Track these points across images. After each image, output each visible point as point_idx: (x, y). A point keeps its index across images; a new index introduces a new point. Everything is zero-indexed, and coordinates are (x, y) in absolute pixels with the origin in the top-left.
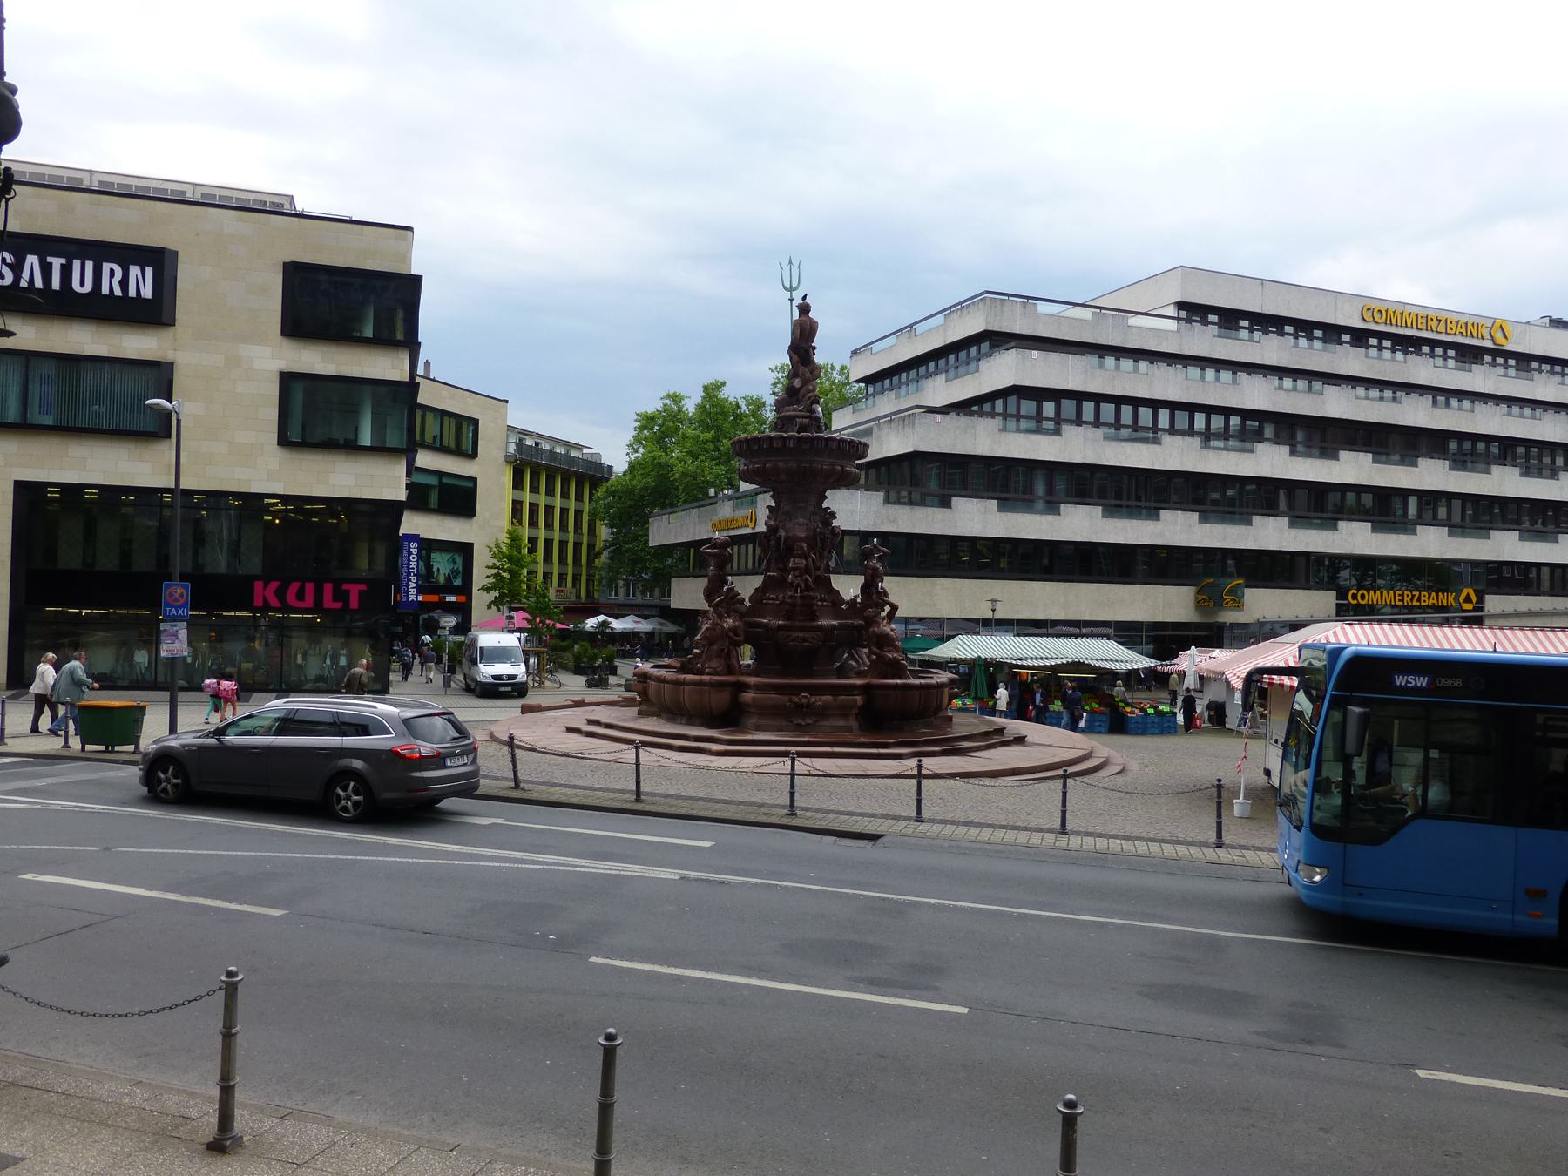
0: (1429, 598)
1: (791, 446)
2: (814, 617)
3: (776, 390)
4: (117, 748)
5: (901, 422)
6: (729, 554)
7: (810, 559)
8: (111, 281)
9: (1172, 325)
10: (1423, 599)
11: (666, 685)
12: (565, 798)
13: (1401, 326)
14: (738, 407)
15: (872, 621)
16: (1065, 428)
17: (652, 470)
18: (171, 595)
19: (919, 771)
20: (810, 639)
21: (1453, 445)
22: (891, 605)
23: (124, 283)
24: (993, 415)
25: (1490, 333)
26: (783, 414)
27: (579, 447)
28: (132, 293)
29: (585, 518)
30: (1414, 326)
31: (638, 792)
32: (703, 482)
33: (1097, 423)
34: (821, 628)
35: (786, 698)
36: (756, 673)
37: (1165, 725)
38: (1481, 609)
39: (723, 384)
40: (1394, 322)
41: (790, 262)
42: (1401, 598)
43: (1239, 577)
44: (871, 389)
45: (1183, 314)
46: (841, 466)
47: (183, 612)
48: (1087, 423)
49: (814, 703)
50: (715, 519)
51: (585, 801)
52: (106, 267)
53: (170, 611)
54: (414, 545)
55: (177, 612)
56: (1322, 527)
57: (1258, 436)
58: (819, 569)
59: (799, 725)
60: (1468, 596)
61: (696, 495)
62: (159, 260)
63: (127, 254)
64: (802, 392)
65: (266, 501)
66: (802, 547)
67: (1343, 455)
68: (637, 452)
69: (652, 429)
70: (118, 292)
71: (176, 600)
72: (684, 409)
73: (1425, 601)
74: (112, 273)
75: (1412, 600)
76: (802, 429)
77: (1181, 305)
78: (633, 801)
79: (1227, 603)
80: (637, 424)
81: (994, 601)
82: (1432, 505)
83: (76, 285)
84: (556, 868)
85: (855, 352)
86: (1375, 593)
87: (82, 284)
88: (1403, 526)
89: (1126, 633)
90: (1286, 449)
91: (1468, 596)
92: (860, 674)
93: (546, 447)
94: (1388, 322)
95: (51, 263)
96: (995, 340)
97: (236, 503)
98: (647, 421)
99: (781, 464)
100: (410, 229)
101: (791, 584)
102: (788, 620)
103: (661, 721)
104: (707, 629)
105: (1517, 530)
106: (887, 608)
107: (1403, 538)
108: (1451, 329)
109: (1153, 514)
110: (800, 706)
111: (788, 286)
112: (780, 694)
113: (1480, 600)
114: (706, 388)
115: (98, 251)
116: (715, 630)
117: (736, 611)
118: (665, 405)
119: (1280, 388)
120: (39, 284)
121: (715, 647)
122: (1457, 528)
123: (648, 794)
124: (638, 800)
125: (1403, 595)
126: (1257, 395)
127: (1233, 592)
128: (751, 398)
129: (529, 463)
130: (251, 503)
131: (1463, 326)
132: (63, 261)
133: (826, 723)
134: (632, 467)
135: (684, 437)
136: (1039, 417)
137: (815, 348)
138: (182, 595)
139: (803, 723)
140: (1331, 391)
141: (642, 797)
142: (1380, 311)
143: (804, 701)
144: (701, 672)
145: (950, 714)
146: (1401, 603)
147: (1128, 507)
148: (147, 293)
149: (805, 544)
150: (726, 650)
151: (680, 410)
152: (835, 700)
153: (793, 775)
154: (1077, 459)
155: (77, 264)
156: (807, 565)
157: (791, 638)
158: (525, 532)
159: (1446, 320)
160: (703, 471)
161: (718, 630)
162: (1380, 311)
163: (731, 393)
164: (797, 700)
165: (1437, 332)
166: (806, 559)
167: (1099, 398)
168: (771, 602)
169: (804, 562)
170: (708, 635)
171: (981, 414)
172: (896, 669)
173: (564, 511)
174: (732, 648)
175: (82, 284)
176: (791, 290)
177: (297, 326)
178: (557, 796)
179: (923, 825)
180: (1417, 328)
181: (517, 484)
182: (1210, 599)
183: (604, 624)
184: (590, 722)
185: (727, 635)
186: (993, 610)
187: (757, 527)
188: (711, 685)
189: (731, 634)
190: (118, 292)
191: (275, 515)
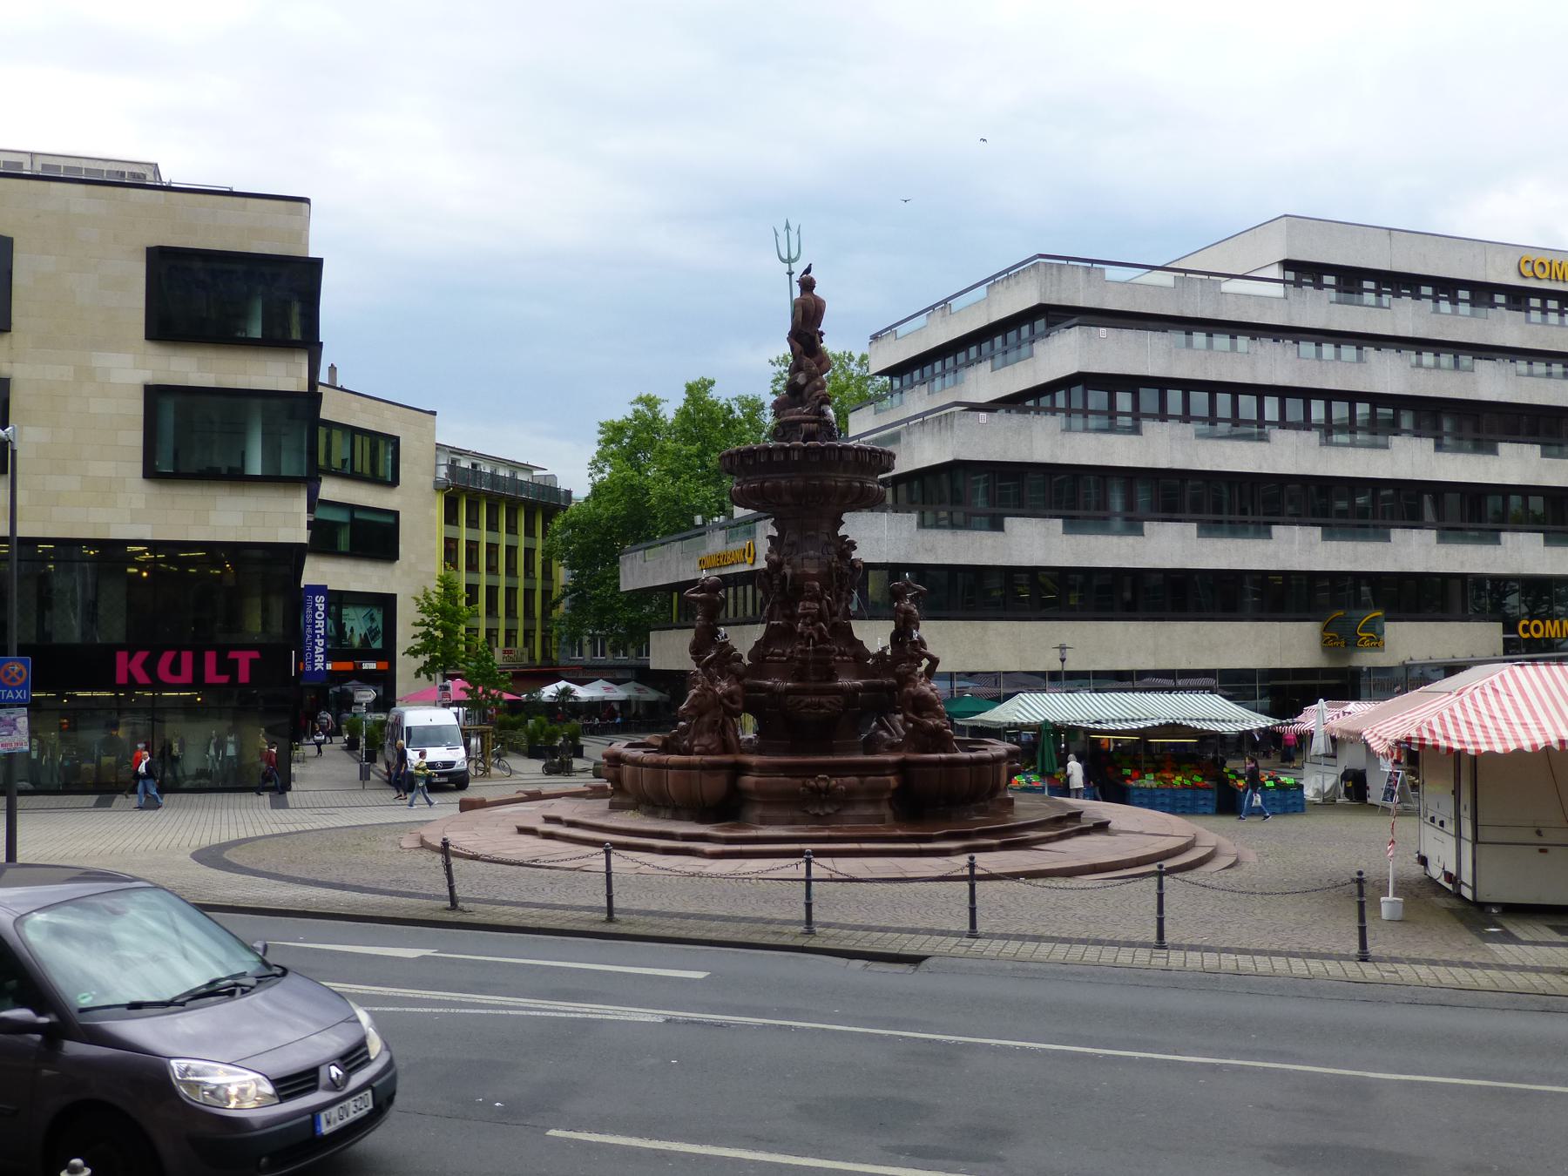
1: (796, 458)
2: (831, 675)
3: (778, 388)
5: (936, 423)
6: (721, 598)
7: (824, 602)
9: (1277, 290)
11: (644, 769)
14: (731, 411)
15: (906, 679)
16: (1146, 424)
17: (622, 494)
18: (7, 673)
19: (972, 871)
20: (828, 705)
22: (930, 657)
24: (1053, 410)
26: (784, 419)
27: (528, 468)
29: (539, 558)
31: (610, 909)
32: (687, 507)
33: (1186, 417)
34: (841, 690)
35: (799, 781)
36: (759, 751)
37: (1289, 802)
39: (712, 383)
40: (1560, 277)
41: (788, 227)
43: (1377, 607)
44: (897, 383)
45: (1291, 276)
46: (860, 482)
48: (1173, 417)
50: (704, 554)
51: (542, 924)
53: (6, 694)
54: (320, 600)
55: (15, 694)
57: (1394, 428)
59: (817, 815)
64: (807, 390)
65: (130, 549)
66: (814, 588)
69: (620, 442)
71: (13, 680)
72: (661, 415)
76: (810, 436)
77: (1287, 265)
79: (1363, 642)
80: (601, 437)
81: (1062, 648)
84: (504, 1012)
85: (875, 337)
86: (1552, 625)
89: (1235, 684)
90: (1429, 443)
92: (893, 748)
93: (486, 469)
94: (1553, 277)
96: (1053, 316)
97: (92, 553)
98: (614, 433)
99: (783, 482)
100: (306, 200)
101: (801, 634)
102: (799, 680)
103: (639, 816)
104: (695, 695)
106: (925, 662)
109: (1262, 530)
110: (816, 791)
111: (785, 257)
112: (791, 777)
114: (690, 389)
117: (731, 672)
118: (636, 411)
119: (1419, 365)
121: (706, 719)
123: (623, 911)
124: (610, 919)
128: (746, 399)
129: (465, 490)
130: (112, 551)
133: (851, 812)
134: (597, 491)
135: (662, 451)
136: (1112, 412)
137: (822, 334)
138: (20, 673)
139: (822, 814)
140: (1484, 367)
143: (822, 784)
144: (689, 752)
145: (1010, 796)
147: (1230, 522)
149: (817, 583)
150: (720, 721)
151: (655, 418)
152: (862, 782)
153: (808, 881)
154: (1163, 463)
156: (820, 610)
157: (802, 704)
158: (462, 578)
160: (687, 494)
161: (709, 697)
163: (721, 394)
164: (812, 783)
166: (819, 601)
167: (1187, 386)
168: (776, 658)
169: (817, 605)
170: (696, 703)
171: (1038, 410)
172: (938, 740)
173: (511, 550)
174: (727, 719)
176: (790, 261)
178: (506, 918)
181: (451, 518)
182: (1340, 638)
183: (566, 692)
184: (548, 820)
185: (721, 703)
186: (1063, 660)
187: (756, 562)
188: (703, 767)
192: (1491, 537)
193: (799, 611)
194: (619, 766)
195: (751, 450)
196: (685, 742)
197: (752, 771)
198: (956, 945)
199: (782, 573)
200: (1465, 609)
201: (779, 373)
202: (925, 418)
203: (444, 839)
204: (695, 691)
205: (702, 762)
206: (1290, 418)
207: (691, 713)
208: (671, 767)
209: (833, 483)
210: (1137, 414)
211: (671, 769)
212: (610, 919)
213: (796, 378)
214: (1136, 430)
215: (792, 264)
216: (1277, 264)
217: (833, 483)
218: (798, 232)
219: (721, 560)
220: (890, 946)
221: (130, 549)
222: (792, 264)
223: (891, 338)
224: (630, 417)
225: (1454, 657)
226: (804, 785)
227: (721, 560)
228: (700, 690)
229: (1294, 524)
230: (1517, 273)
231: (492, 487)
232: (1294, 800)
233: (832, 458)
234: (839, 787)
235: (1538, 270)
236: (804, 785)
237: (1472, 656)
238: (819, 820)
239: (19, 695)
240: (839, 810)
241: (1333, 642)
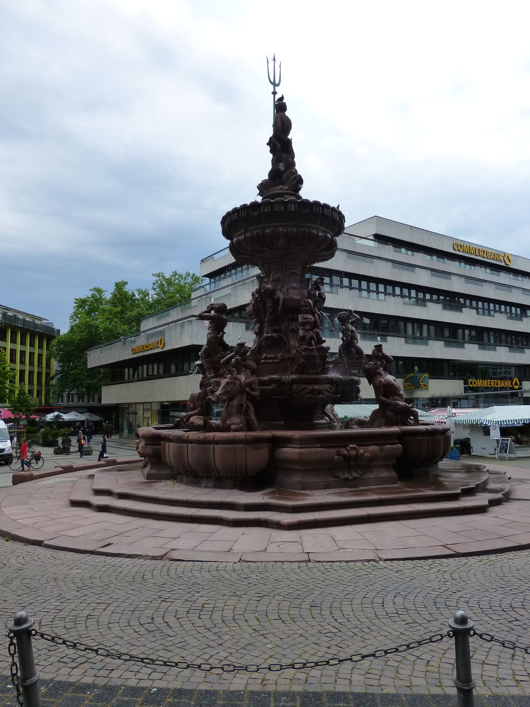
0: (501, 383)
1: (293, 209)
3: (155, 287)
5: (251, 284)
10: (499, 383)
11: (189, 445)
13: (469, 253)
14: (134, 295)
17: (85, 329)
25: (504, 259)
27: (40, 319)
30: (475, 254)
32: (117, 333)
34: (331, 381)
35: (333, 451)
37: (453, 455)
38: (520, 388)
39: (126, 283)
40: (466, 251)
42: (490, 383)
48: (346, 287)
50: (134, 346)
56: (457, 346)
59: (347, 479)
60: (516, 382)
68: (75, 321)
69: (84, 308)
72: (104, 297)
73: (499, 385)
75: (494, 384)
79: (421, 387)
80: (76, 305)
85: (202, 261)
86: (485, 381)
91: (516, 382)
93: (21, 317)
94: (464, 251)
98: (81, 303)
99: (280, 229)
103: (183, 487)
107: (492, 353)
108: (489, 256)
110: (347, 459)
112: (326, 447)
113: (521, 384)
114: (117, 285)
118: (93, 294)
128: (141, 291)
129: (10, 325)
131: (493, 255)
134: (72, 330)
135: (104, 310)
139: (350, 478)
142: (460, 246)
143: (353, 453)
146: (490, 386)
147: (371, 334)
151: (100, 298)
152: (382, 450)
159: (487, 252)
160: (116, 328)
162: (460, 246)
163: (129, 289)
164: (345, 452)
165: (483, 257)
168: (271, 361)
173: (32, 354)
180: (476, 255)
183: (58, 417)
184: (98, 492)
187: (165, 347)
188: (246, 442)
192: (461, 345)
194: (160, 444)
197: (291, 443)
199: (276, 297)
200: (449, 375)
201: (156, 280)
202: (244, 282)
203: (19, 621)
205: (248, 437)
207: (225, 397)
208: (191, 442)
211: (217, 444)
216: (372, 236)
219: (145, 348)
223: (212, 260)
224: (90, 296)
225: (448, 394)
226: (338, 454)
227: (145, 348)
228: (230, 378)
229: (395, 336)
230: (452, 246)
231: (23, 325)
232: (455, 455)
233: (318, 212)
235: (459, 248)
236: (338, 454)
237: (454, 394)
238: (347, 483)
241: (409, 387)
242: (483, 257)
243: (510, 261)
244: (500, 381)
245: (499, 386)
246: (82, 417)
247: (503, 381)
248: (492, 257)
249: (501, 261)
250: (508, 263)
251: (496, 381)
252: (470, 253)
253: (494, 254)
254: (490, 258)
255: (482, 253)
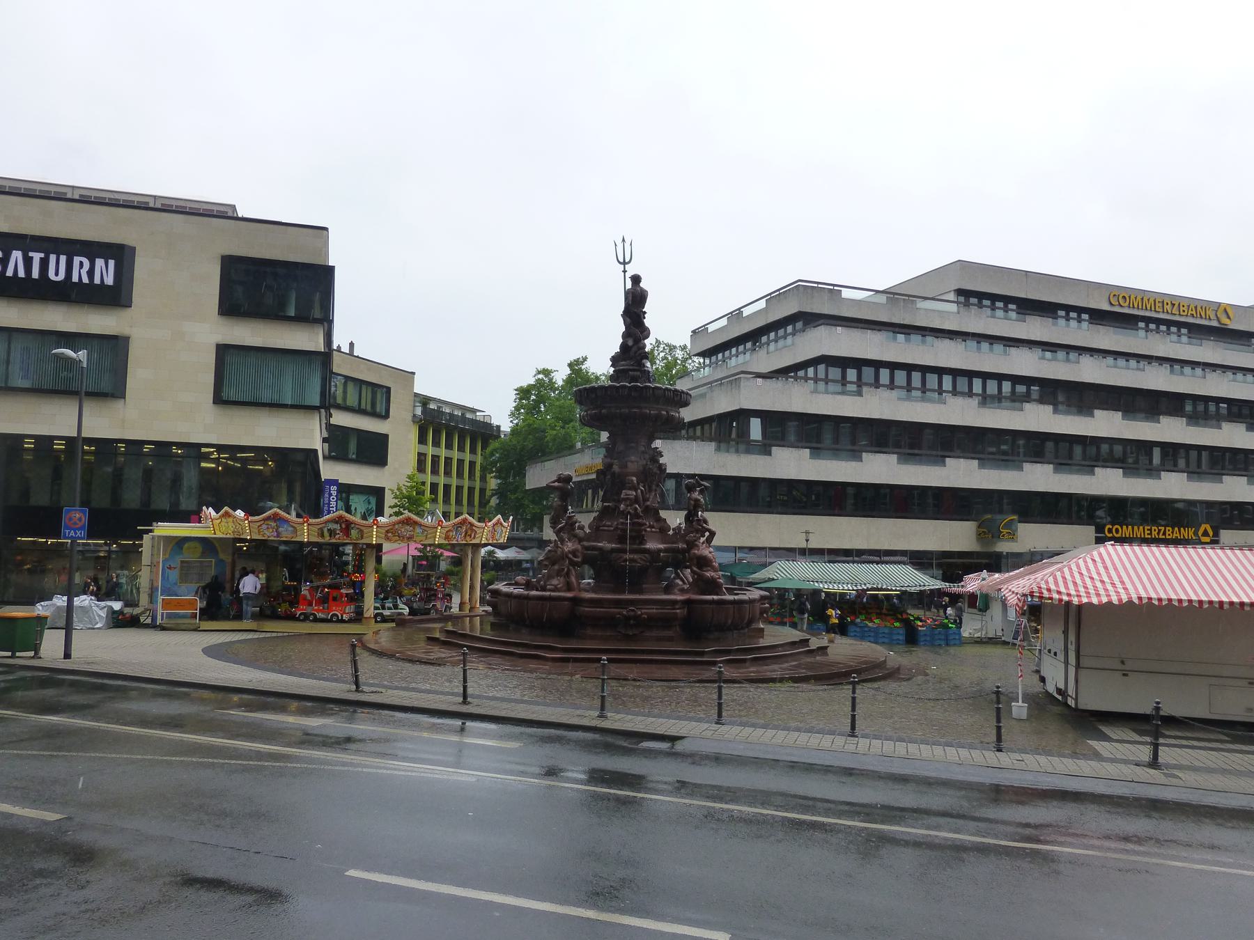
0: (1172, 532)
2: (643, 541)
4: (18, 654)
6: (571, 487)
7: (639, 491)
8: (80, 270)
9: (953, 308)
12: (400, 700)
16: (865, 389)
18: (70, 519)
20: (639, 560)
21: (1189, 408)
23: (91, 273)
24: (806, 379)
25: (1216, 315)
26: (617, 368)
28: (97, 281)
30: (1153, 309)
31: (465, 696)
33: (892, 386)
36: (593, 590)
41: (624, 240)
42: (1149, 532)
43: (1014, 513)
44: (707, 361)
45: (962, 299)
46: (667, 412)
47: (81, 534)
49: (640, 615)
51: (416, 704)
52: (77, 260)
55: (76, 533)
57: (1027, 398)
58: (648, 501)
60: (1206, 530)
61: (565, 448)
62: (121, 254)
63: (93, 250)
64: (634, 349)
66: (632, 480)
67: (1097, 413)
70: (85, 280)
73: (1169, 535)
74: (81, 264)
75: (1158, 534)
76: (634, 379)
77: (960, 292)
78: (460, 703)
79: (1003, 536)
81: (807, 533)
82: (1174, 455)
83: (52, 275)
84: (375, 771)
86: (1127, 528)
87: (57, 274)
88: (1152, 472)
89: (919, 560)
90: (1050, 408)
91: (1206, 530)
95: (32, 257)
96: (807, 319)
97: (180, 452)
100: (326, 229)
101: (623, 511)
102: (620, 543)
104: (549, 551)
105: (1245, 476)
107: (1150, 482)
108: (1184, 311)
109: (940, 460)
111: (622, 260)
113: (1216, 534)
115: (70, 247)
116: (556, 552)
119: (1043, 358)
120: (21, 274)
121: (556, 567)
122: (1195, 473)
123: (473, 696)
124: (465, 702)
125: (1151, 530)
126: (1025, 363)
127: (1009, 525)
130: (194, 450)
132: (42, 255)
133: (648, 634)
136: (844, 381)
137: (645, 313)
138: (80, 519)
140: (1086, 360)
141: (469, 699)
142: (1124, 297)
144: (544, 589)
146: (1150, 536)
148: (109, 280)
149: (634, 479)
150: (566, 570)
151: (551, 380)
155: (53, 258)
156: (636, 496)
157: (622, 559)
159: (1179, 304)
161: (559, 553)
162: (1124, 297)
165: (1172, 313)
166: (636, 490)
167: (893, 366)
169: (634, 493)
170: (549, 556)
171: (796, 378)
174: (571, 568)
175: (57, 274)
176: (624, 263)
177: (230, 307)
179: (723, 728)
180: (1155, 311)
182: (988, 532)
185: (567, 557)
186: (807, 541)
189: (570, 556)
190: (85, 280)
191: (213, 461)
193: (622, 496)
195: (593, 387)
196: (542, 582)
198: (706, 729)
204: (549, 548)
206: (959, 389)
209: (648, 412)
210: (860, 383)
212: (465, 702)
213: (627, 341)
214: (860, 394)
215: (626, 266)
217: (648, 412)
218: (631, 244)
220: (658, 728)
221: (204, 450)
222: (626, 266)
234: (643, 616)
239: (78, 534)
240: (642, 632)
242: (1172, 313)
243: (1229, 317)
244: (1170, 529)
245: (1167, 537)
246: (524, 555)
247: (1176, 529)
248: (1190, 312)
249: (1210, 319)
250: (1225, 320)
251: (1163, 528)
252: (1144, 308)
253: (1196, 307)
254: (1187, 315)
255: (1169, 307)
